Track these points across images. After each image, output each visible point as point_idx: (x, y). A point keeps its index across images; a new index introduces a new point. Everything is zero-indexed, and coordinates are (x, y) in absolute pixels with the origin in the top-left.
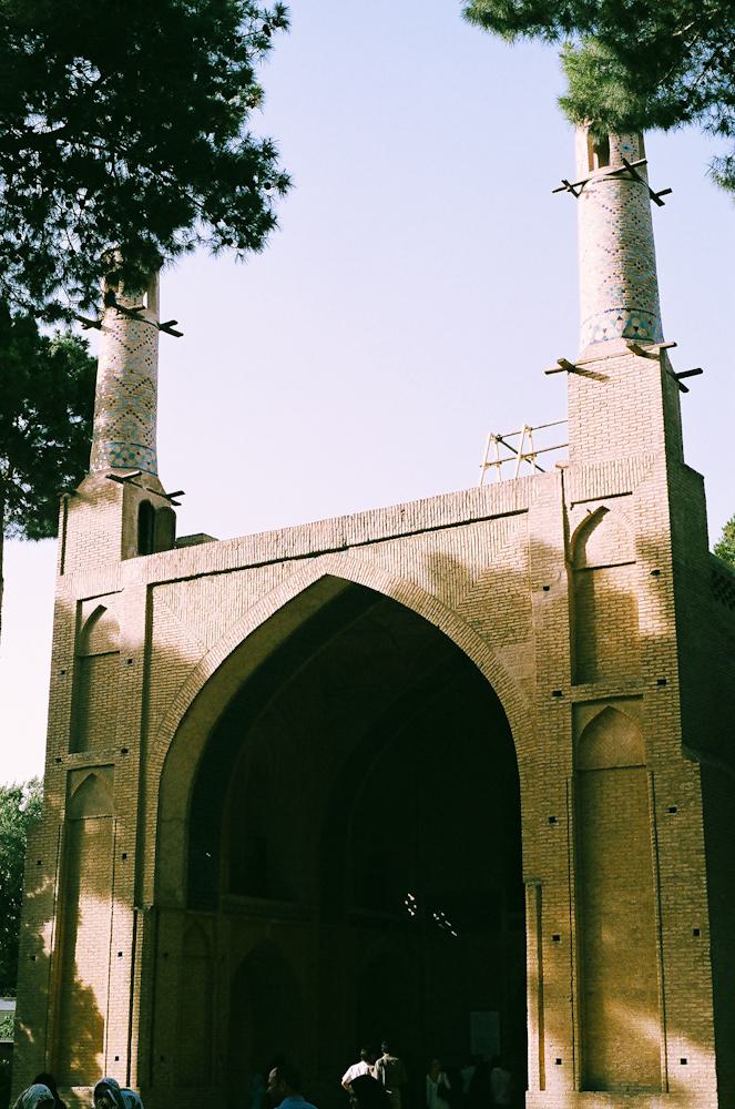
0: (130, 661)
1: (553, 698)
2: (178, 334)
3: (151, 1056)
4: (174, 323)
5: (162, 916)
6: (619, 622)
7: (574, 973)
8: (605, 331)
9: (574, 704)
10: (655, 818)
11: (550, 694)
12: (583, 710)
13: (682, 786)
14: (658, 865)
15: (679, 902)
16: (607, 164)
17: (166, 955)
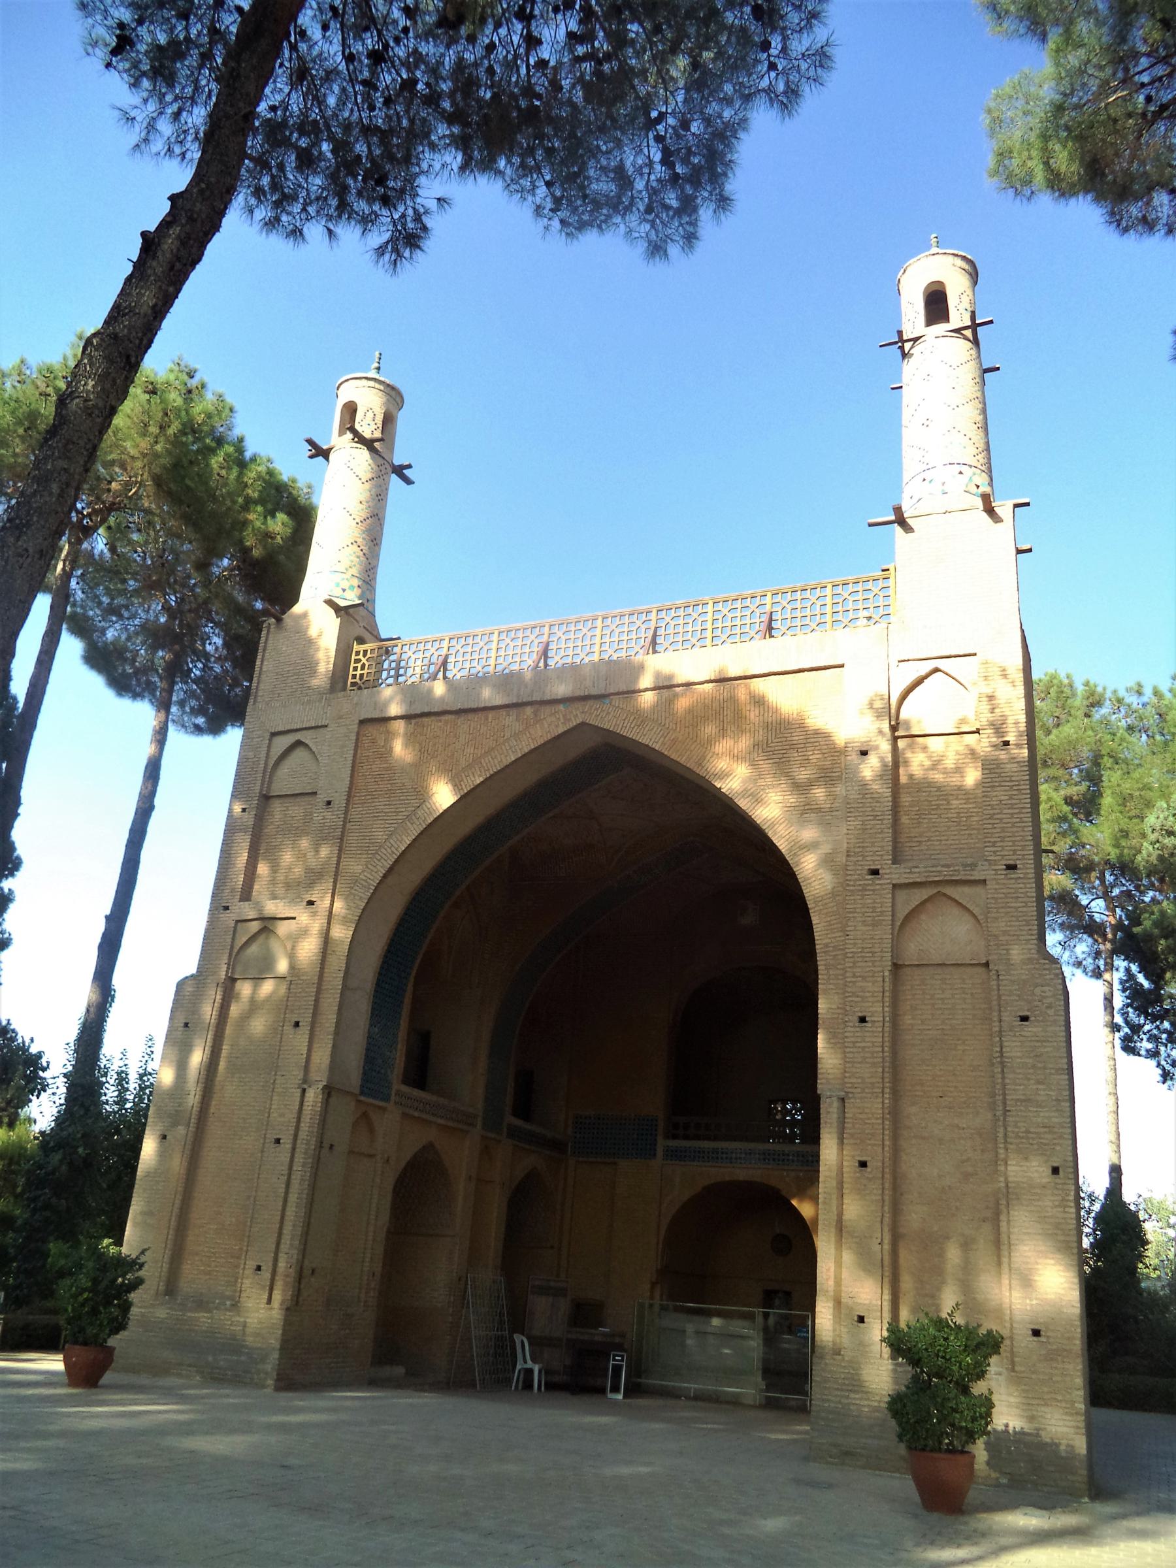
0: (329, 803)
1: (870, 877)
2: (408, 481)
3: (301, 1268)
4: (409, 466)
5: (333, 1100)
6: (951, 798)
7: (886, 1208)
8: (943, 484)
9: (894, 886)
10: (1001, 1027)
11: (865, 872)
12: (902, 895)
13: (1038, 991)
14: (1004, 1085)
15: (1032, 1130)
16: (946, 318)
17: (331, 1146)
